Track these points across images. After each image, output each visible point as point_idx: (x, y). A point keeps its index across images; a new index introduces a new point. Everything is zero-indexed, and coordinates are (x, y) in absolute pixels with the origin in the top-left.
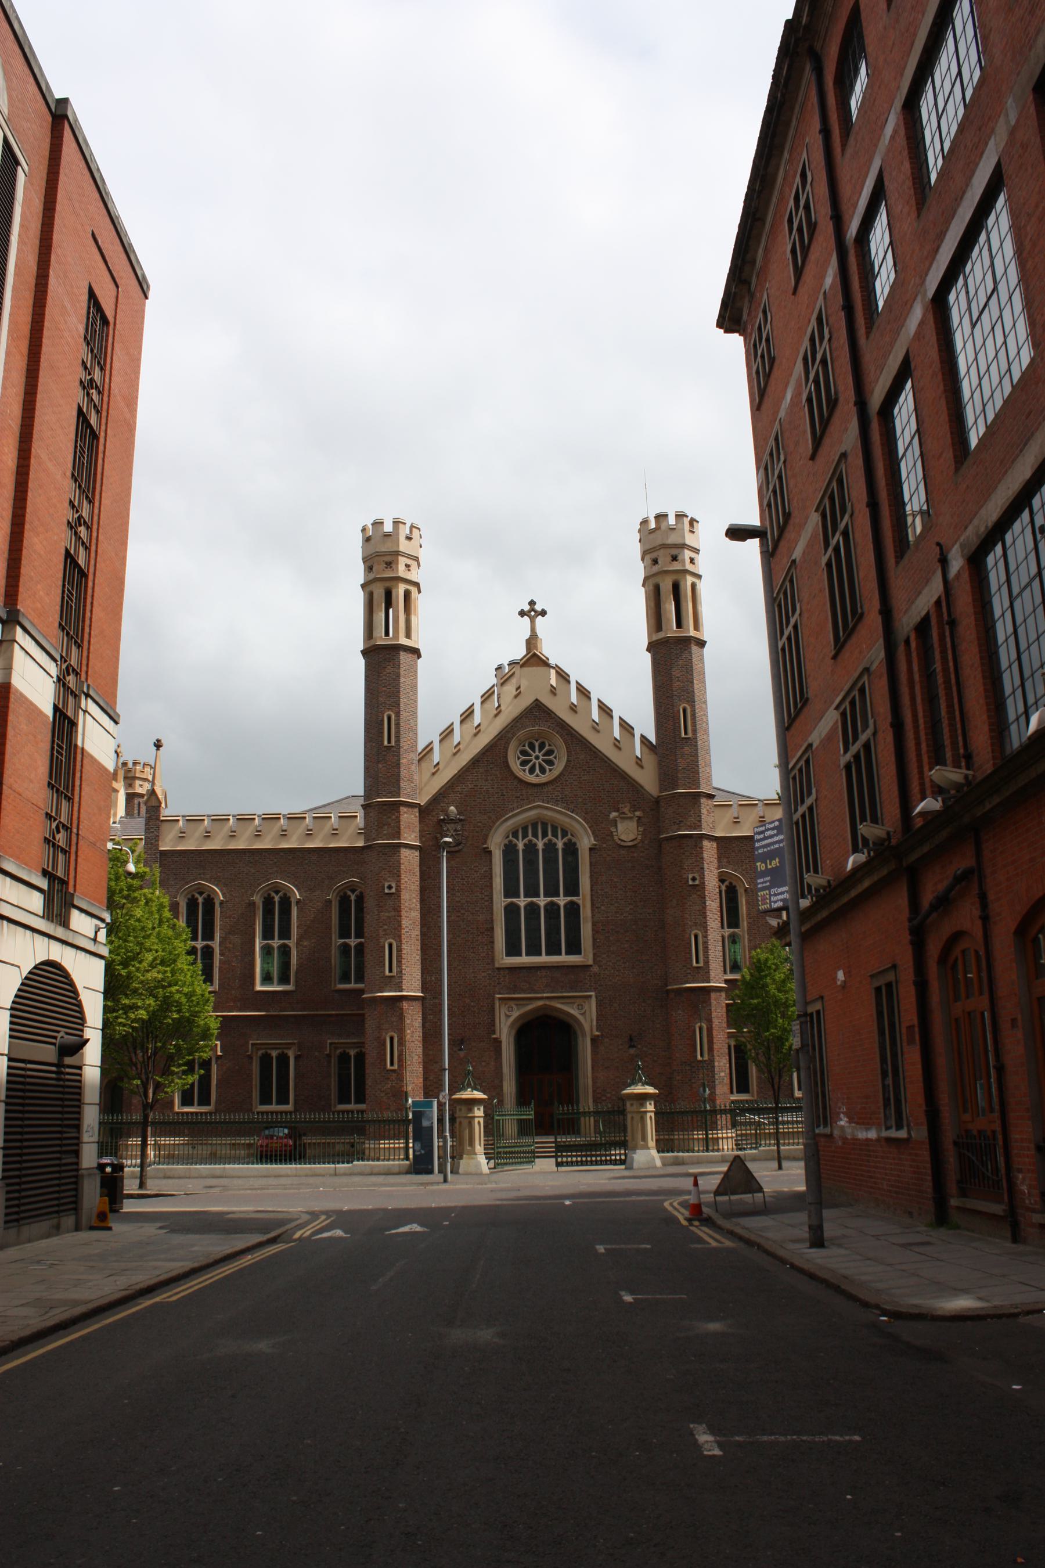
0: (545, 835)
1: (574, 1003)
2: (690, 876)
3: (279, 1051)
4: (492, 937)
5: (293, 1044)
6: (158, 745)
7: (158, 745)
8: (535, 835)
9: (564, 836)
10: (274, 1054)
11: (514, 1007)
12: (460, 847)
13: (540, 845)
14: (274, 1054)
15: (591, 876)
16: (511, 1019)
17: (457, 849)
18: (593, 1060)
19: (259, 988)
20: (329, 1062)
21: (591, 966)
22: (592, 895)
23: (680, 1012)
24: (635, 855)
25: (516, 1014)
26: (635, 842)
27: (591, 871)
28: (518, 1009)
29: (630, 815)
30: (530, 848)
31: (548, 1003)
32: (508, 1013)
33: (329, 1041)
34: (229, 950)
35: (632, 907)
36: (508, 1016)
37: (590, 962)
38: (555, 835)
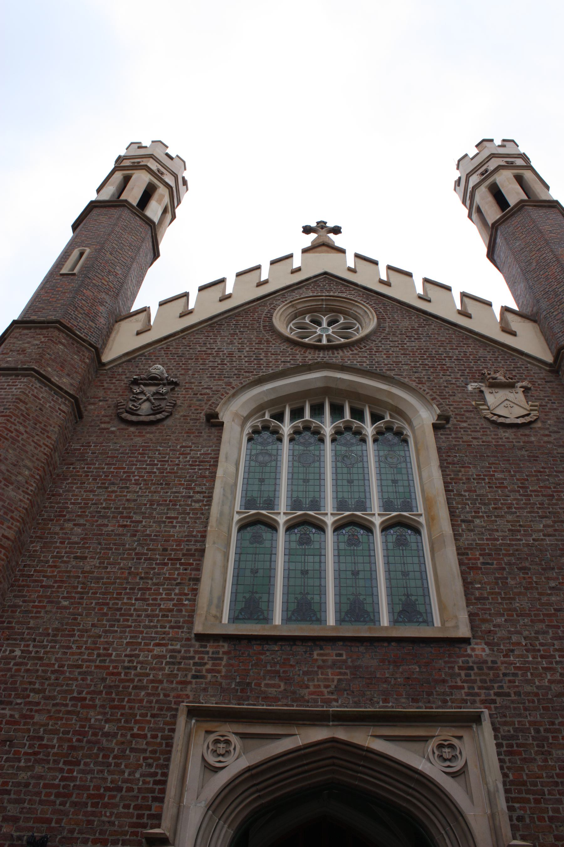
1: (425, 739)
4: (199, 569)
9: (375, 418)
11: (234, 739)
12: (159, 416)
15: (443, 467)
16: (223, 778)
17: (152, 418)
21: (466, 641)
22: (449, 501)
24: (533, 439)
26: (528, 419)
27: (441, 460)
28: (245, 751)
31: (341, 734)
32: (212, 760)
35: (549, 522)
37: (464, 631)
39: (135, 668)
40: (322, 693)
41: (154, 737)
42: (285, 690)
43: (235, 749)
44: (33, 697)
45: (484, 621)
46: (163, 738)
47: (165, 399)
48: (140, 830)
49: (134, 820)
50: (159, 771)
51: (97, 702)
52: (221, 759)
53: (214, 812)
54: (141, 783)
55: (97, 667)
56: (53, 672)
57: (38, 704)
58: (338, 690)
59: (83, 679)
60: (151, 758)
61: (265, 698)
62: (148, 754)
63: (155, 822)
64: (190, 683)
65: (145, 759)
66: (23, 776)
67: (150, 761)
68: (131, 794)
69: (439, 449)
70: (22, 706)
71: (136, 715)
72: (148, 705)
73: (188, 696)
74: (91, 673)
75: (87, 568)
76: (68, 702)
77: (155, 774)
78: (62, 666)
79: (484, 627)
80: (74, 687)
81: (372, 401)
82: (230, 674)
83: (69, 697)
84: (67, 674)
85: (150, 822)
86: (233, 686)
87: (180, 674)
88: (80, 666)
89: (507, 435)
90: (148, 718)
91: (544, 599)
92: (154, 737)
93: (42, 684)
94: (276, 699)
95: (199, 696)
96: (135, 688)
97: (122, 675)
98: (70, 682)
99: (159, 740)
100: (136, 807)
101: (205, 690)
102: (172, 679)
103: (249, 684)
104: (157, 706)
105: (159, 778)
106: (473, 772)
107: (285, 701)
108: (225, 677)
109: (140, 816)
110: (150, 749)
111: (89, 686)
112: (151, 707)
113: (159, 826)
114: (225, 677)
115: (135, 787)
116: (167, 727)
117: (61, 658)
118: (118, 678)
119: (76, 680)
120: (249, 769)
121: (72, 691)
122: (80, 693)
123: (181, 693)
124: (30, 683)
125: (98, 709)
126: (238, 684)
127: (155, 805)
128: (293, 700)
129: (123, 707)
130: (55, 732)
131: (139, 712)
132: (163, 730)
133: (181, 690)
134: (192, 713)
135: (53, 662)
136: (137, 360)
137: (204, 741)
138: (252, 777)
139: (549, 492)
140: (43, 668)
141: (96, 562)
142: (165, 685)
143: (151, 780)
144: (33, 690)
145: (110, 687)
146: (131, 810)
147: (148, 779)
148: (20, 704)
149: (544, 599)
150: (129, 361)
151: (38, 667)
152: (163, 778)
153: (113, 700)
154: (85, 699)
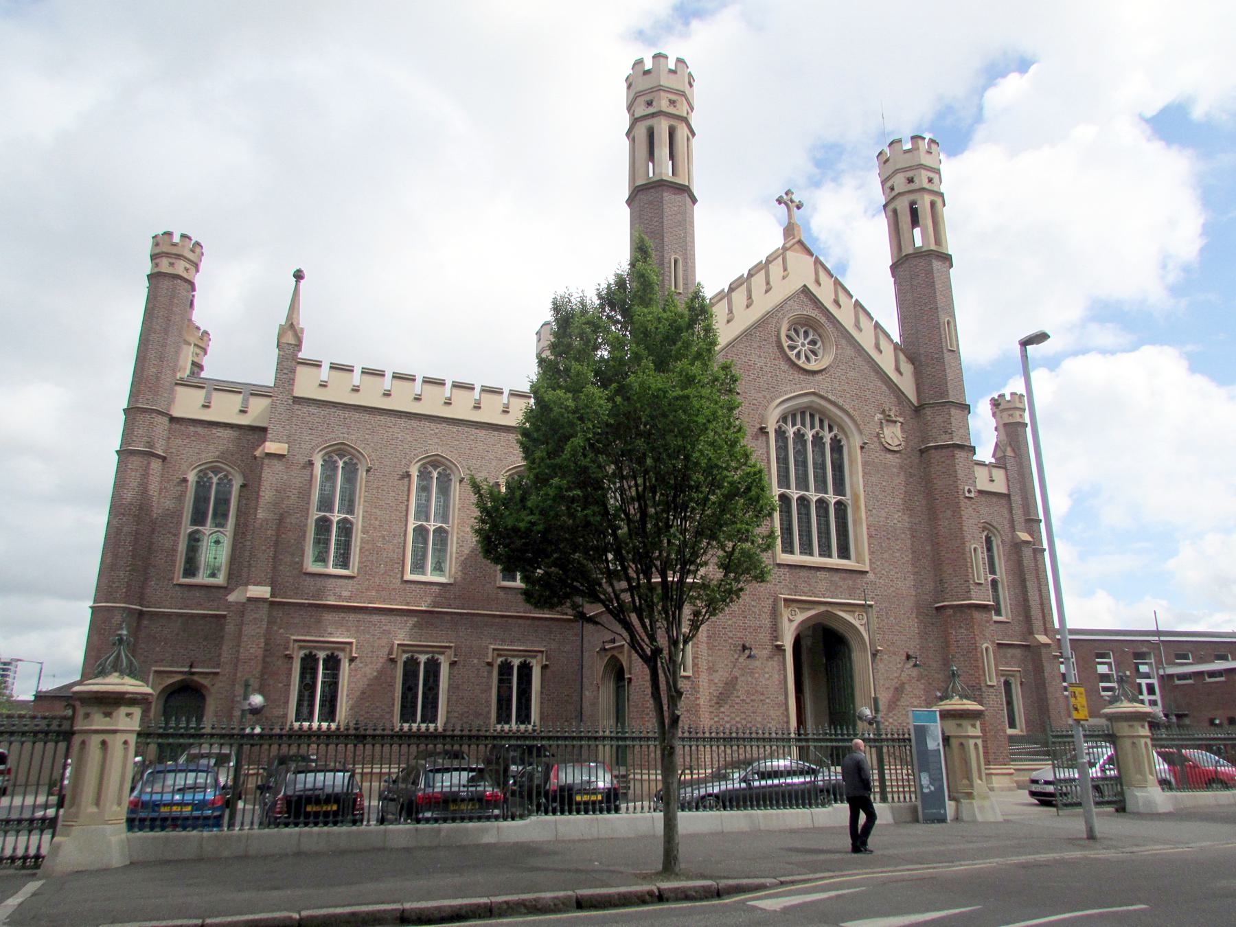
0: (812, 427)
1: (854, 612)
2: (966, 488)
3: (429, 656)
5: (449, 647)
6: (299, 276)
7: (299, 276)
8: (803, 424)
10: (423, 658)
11: (797, 610)
13: (809, 435)
14: (423, 658)
19: (409, 576)
20: (490, 672)
21: (867, 572)
23: (963, 630)
25: (800, 617)
29: (894, 419)
30: (799, 436)
32: (791, 617)
33: (492, 647)
34: (375, 528)
35: (900, 514)
36: (790, 621)
37: (867, 569)
38: (822, 427)
66: (730, 622)
81: (829, 419)
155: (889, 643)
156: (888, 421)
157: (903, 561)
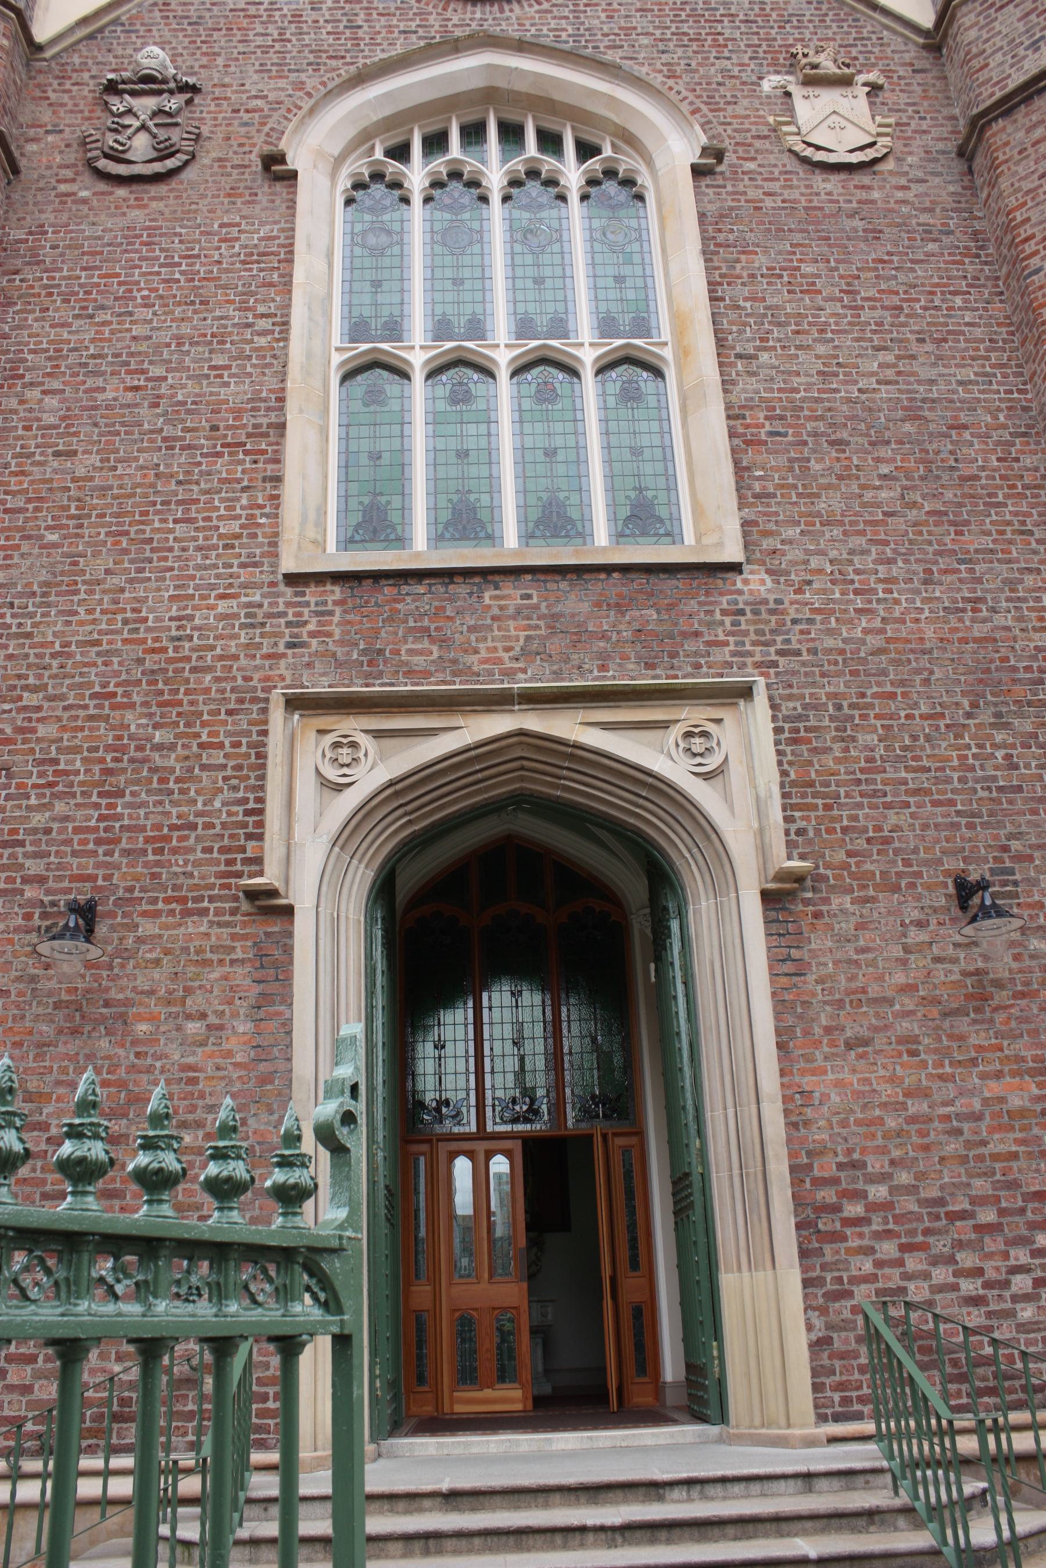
1: (664, 725)
11: (364, 740)
12: (171, 163)
15: (707, 255)
17: (158, 167)
18: (781, 1006)
21: (735, 568)
22: (715, 319)
24: (876, 195)
26: (870, 154)
28: (383, 756)
31: (534, 722)
32: (332, 774)
35: (890, 358)
37: (733, 553)
39: (190, 638)
40: (499, 661)
41: (237, 745)
42: (440, 657)
43: (366, 755)
44: (30, 699)
45: (766, 534)
46: (249, 746)
47: (177, 124)
48: (233, 881)
49: (222, 868)
50: (251, 796)
51: (135, 698)
52: (345, 771)
53: (342, 848)
54: (224, 815)
55: (125, 641)
56: (53, 656)
57: (39, 708)
58: (526, 653)
59: (105, 664)
60: (235, 777)
61: (408, 673)
62: (229, 772)
63: (254, 868)
64: (284, 655)
65: (225, 779)
66: (38, 819)
67: (234, 782)
68: (212, 832)
69: (702, 216)
70: (14, 714)
71: (201, 714)
72: (219, 696)
73: (283, 678)
74: (117, 652)
75: (81, 472)
76: (87, 701)
77: (245, 801)
78: (67, 644)
79: (767, 543)
80: (93, 678)
81: (578, 116)
82: (347, 637)
83: (88, 693)
84: (78, 657)
85: (246, 869)
86: (355, 656)
87: (265, 641)
88: (97, 643)
89: (829, 186)
90: (223, 717)
91: (868, 496)
92: (237, 745)
93: (40, 677)
94: (426, 674)
95: (301, 675)
96: (194, 670)
97: (170, 651)
98: (86, 670)
99: (244, 749)
100: (222, 850)
101: (309, 665)
102: (253, 652)
103: (380, 652)
104: (234, 696)
105: (251, 805)
106: (736, 771)
107: (440, 676)
108: (341, 643)
109: (229, 862)
110: (231, 763)
111: (117, 674)
112: (224, 699)
113: (261, 873)
114: (341, 643)
115: (217, 822)
116: (254, 729)
117: (63, 632)
118: (163, 656)
119: (95, 664)
120: (391, 784)
121: (90, 685)
122: (105, 685)
123: (271, 673)
124: (19, 677)
125: (139, 709)
126: (364, 652)
127: (251, 845)
128: (455, 674)
129: (180, 703)
130: (76, 750)
131: (206, 709)
132: (248, 734)
133: (271, 668)
134: (293, 703)
135: (50, 639)
136: (107, 34)
137: (317, 746)
138: (397, 794)
139: (895, 300)
140: (37, 651)
141: (95, 459)
142: (243, 662)
143: (240, 809)
144: (26, 688)
145: (153, 672)
146: (215, 855)
147: (234, 809)
148: (10, 711)
149: (868, 496)
150: (91, 37)
151: (27, 650)
152: (259, 806)
153: (161, 693)
154: (114, 695)
155: (861, 844)
156: (809, 82)
157: (912, 515)
